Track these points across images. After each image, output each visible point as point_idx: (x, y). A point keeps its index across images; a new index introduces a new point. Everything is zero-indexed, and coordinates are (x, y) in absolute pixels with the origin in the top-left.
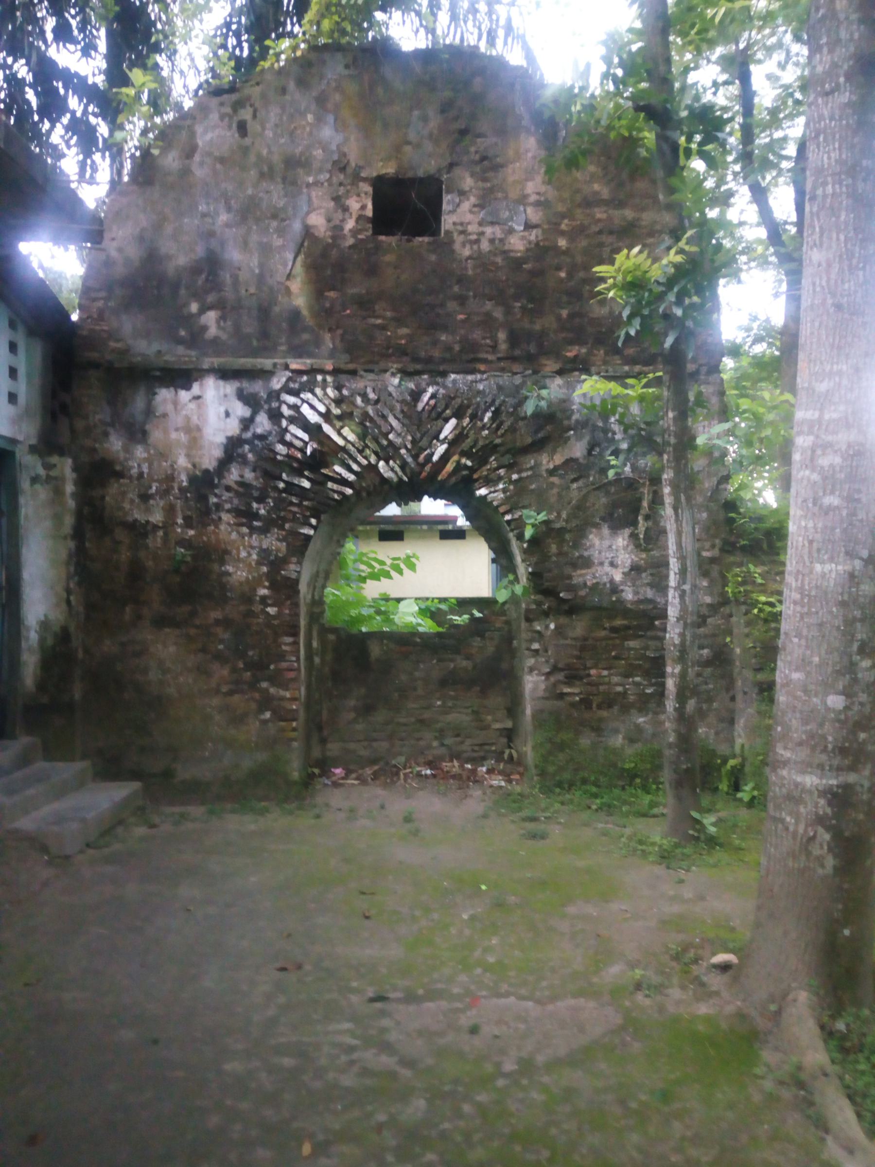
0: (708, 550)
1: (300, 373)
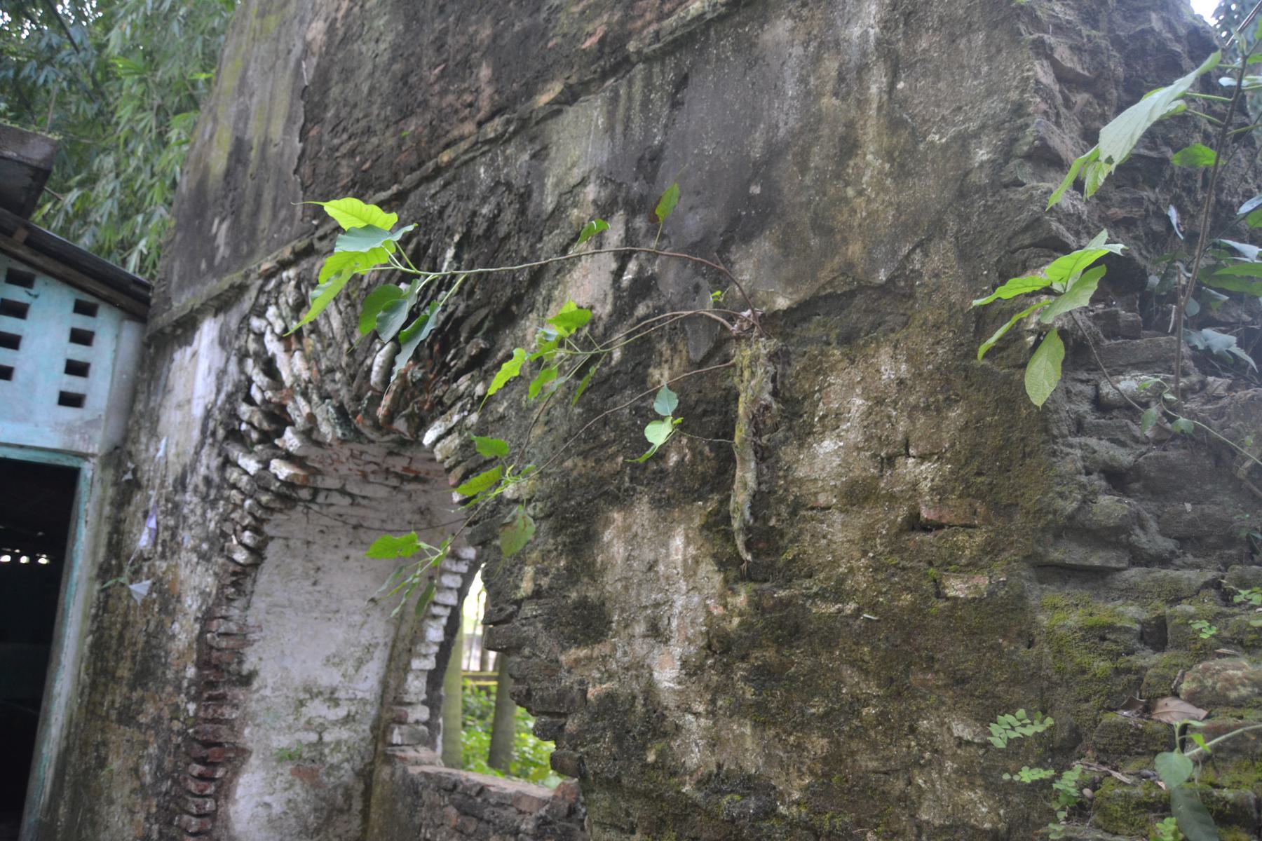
0: (973, 566)
1: (268, 275)
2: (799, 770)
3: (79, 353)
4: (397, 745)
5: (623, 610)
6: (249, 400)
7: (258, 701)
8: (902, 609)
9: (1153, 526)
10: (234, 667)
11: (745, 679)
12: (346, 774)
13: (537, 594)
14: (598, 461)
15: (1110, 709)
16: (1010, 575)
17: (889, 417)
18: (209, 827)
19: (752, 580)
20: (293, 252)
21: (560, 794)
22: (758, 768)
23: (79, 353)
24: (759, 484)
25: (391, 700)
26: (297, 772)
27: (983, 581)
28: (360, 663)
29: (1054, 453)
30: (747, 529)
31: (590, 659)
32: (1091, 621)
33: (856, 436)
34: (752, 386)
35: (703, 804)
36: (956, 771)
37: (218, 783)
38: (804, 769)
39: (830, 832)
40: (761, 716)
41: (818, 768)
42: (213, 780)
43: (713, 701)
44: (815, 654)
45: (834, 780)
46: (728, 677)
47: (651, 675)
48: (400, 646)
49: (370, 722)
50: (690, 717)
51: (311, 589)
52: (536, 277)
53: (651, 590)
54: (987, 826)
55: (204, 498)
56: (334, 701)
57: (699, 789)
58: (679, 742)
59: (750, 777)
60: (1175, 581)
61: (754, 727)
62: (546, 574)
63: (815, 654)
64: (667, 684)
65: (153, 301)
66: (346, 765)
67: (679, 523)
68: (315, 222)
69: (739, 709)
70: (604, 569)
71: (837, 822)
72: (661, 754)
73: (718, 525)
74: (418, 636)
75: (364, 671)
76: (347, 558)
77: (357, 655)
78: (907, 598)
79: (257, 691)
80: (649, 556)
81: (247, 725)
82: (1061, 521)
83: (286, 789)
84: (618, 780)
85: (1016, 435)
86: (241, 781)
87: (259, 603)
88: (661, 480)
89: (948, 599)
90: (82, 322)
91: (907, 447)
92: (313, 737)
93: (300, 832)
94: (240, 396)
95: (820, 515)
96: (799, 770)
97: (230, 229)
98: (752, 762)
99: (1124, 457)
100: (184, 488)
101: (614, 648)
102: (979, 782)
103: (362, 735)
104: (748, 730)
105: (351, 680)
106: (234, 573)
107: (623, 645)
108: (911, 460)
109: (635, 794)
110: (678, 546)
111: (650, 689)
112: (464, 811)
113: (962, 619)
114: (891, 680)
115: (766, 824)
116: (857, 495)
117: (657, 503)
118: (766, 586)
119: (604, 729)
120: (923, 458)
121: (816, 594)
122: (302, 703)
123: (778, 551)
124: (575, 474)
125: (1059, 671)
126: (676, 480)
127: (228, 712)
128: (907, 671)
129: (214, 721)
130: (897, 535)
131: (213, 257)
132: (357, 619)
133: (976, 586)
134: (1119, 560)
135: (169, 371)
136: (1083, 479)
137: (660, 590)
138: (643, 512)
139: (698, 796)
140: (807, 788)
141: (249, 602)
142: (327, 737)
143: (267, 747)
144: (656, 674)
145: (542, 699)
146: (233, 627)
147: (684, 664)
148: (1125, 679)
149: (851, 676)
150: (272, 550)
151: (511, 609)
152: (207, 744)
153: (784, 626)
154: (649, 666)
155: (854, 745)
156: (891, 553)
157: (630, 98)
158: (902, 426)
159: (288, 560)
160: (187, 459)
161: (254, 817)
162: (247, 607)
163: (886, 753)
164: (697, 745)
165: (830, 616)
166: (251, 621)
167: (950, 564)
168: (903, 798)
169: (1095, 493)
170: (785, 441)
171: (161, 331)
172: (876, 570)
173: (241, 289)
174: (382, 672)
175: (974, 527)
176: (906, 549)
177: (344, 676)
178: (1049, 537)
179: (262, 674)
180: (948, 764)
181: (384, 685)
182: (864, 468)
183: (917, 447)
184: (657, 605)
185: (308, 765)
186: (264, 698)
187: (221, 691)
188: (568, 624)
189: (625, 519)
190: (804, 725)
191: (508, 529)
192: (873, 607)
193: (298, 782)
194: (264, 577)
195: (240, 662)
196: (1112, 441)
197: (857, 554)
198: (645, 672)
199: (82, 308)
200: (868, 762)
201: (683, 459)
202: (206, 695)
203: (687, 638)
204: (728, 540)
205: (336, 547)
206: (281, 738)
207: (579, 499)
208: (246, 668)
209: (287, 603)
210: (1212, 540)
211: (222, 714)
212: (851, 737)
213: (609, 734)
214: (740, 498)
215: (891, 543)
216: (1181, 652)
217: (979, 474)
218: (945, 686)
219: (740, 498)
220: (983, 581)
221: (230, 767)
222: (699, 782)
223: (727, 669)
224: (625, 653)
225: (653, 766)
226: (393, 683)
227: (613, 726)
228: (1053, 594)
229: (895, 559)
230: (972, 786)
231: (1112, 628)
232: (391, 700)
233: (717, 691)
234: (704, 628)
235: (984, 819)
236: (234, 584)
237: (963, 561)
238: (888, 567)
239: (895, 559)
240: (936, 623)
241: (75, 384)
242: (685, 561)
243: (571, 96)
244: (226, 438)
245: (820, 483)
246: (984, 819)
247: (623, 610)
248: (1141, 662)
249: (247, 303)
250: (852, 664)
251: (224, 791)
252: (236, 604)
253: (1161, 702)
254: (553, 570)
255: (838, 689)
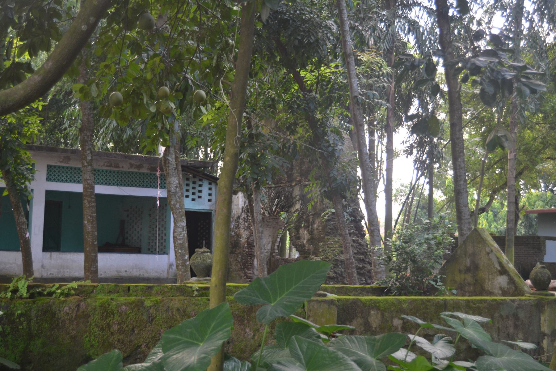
3: (210, 192)
23: (210, 192)
34: (311, 220)
52: (293, 204)
55: (244, 221)
74: (276, 240)
90: (210, 186)
107: (301, 240)
116: (317, 229)
153: (312, 238)
160: (240, 214)
199: (210, 184)
232: (273, 249)
241: (210, 198)
243: (296, 185)
251: (253, 261)
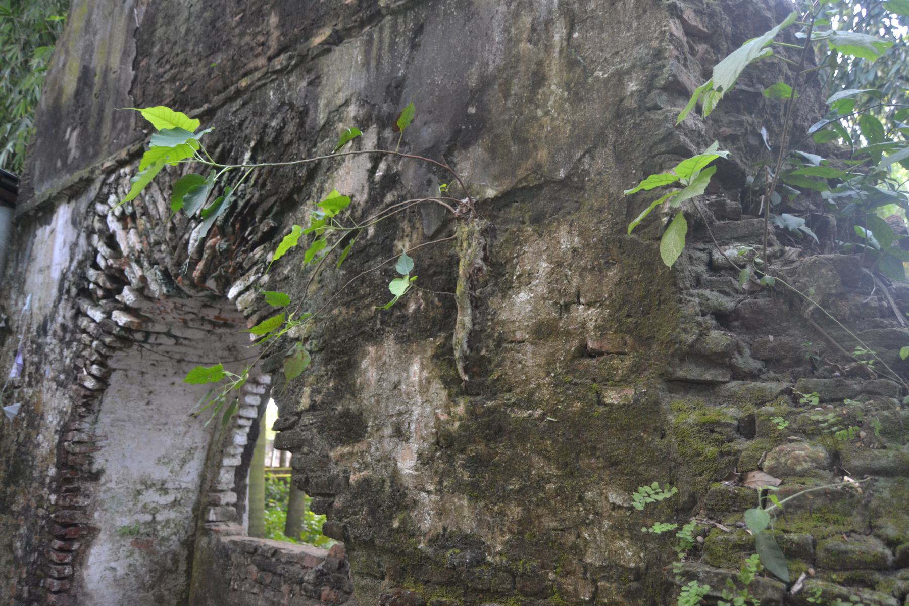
1: (109, 172)
2: (501, 530)
4: (213, 521)
5: (375, 418)
6: (96, 266)
7: (105, 492)
8: (574, 413)
9: (747, 352)
10: (86, 466)
11: (463, 466)
12: (174, 544)
13: (313, 407)
14: (357, 309)
15: (716, 481)
16: (649, 387)
17: (566, 276)
18: (68, 586)
19: (468, 394)
20: (128, 154)
21: (333, 553)
22: (472, 530)
24: (474, 325)
25: (208, 488)
26: (136, 543)
27: (630, 392)
28: (184, 462)
29: (680, 301)
30: (465, 358)
31: (351, 454)
32: (704, 419)
33: (542, 290)
34: (469, 254)
35: (433, 556)
36: (611, 527)
37: (74, 553)
38: (505, 529)
39: (523, 573)
40: (475, 492)
41: (515, 528)
42: (71, 551)
43: (440, 483)
44: (513, 447)
45: (526, 536)
46: (451, 465)
47: (396, 465)
48: (214, 448)
49: (192, 505)
50: (424, 494)
51: (145, 407)
53: (396, 403)
54: (632, 565)
55: (61, 340)
56: (164, 491)
57: (430, 546)
58: (416, 512)
59: (466, 535)
60: (762, 390)
61: (470, 500)
62: (320, 393)
63: (513, 447)
64: (407, 471)
65: (20, 191)
66: (173, 537)
67: (416, 354)
68: (145, 131)
69: (459, 488)
70: (362, 388)
71: (528, 566)
72: (403, 522)
73: (444, 355)
74: (228, 441)
75: (187, 467)
76: (173, 384)
77: (182, 456)
78: (578, 405)
79: (104, 484)
80: (394, 378)
81: (97, 510)
82: (685, 349)
83: (127, 557)
84: (372, 541)
85: (654, 288)
86: (92, 551)
87: (105, 419)
88: (403, 322)
89: (606, 405)
91: (578, 297)
92: (148, 517)
93: (139, 588)
94: (89, 263)
95: (517, 347)
96: (501, 530)
97: (80, 135)
98: (468, 525)
99: (728, 303)
100: (46, 333)
101: (369, 446)
102: (627, 534)
103: (186, 515)
104: (465, 503)
105: (177, 475)
106: (85, 397)
108: (581, 307)
109: (384, 551)
110: (415, 370)
111: (395, 475)
112: (262, 568)
113: (616, 419)
114: (566, 464)
115: (478, 569)
116: (543, 332)
117: (400, 340)
118: (479, 398)
119: (362, 505)
120: (589, 305)
121: (514, 404)
122: (139, 493)
123: (488, 373)
124: (341, 318)
125: (683, 455)
126: (414, 323)
127: (81, 501)
128: (577, 458)
129: (70, 507)
130: (572, 360)
131: (67, 158)
132: (182, 429)
133: (626, 396)
134: (724, 375)
135: (33, 244)
136: (700, 319)
137: (403, 403)
138: (390, 346)
139: (430, 551)
140: (507, 542)
141: (97, 418)
142: (159, 517)
143: (112, 526)
144: (399, 464)
145: (317, 484)
146: (84, 437)
147: (420, 456)
148: (726, 459)
149: (538, 461)
150: (114, 379)
151: (293, 419)
152: (65, 525)
153: (491, 427)
154: (394, 458)
155: (540, 511)
156: (567, 373)
157: (381, 41)
158: (575, 282)
159: (127, 386)
160: (48, 311)
161: (103, 578)
162: (96, 421)
163: (563, 516)
164: (429, 514)
165: (524, 419)
166: (99, 432)
167: (607, 380)
168: (574, 548)
169: (708, 329)
170: (492, 294)
171: (26, 214)
172: (556, 386)
173: (87, 182)
174: (200, 468)
175: (625, 354)
176: (577, 371)
177: (171, 472)
178: (677, 360)
179: (108, 472)
180: (606, 523)
181: (203, 478)
182: (548, 312)
183: (585, 297)
184: (400, 414)
185: (145, 538)
186: (109, 489)
187: (76, 485)
188: (336, 429)
189: (377, 352)
190: (505, 498)
191: (290, 359)
192: (554, 412)
193: (137, 551)
194: (109, 399)
195: (91, 463)
196: (721, 292)
197: (543, 374)
198: (392, 462)
200: (550, 523)
201: (419, 307)
202: (64, 489)
203: (422, 438)
204: (451, 366)
205: (164, 376)
206: (123, 519)
207: (343, 337)
208: (95, 467)
209: (126, 418)
210: (787, 361)
211: (77, 502)
212: (538, 505)
213: (365, 508)
214: (460, 335)
215: (567, 366)
216: (764, 440)
217: (628, 316)
218: (604, 467)
219: (460, 335)
220: (630, 392)
221: (83, 541)
222: (430, 541)
223: (450, 459)
224: (377, 449)
225: (398, 531)
226: (209, 476)
227: (368, 502)
228: (679, 401)
229: (570, 378)
230: (622, 537)
231: (718, 423)
232: (207, 488)
233: (443, 475)
234: (434, 430)
235: (630, 560)
236: (84, 405)
237: (617, 378)
238: (565, 383)
239: (570, 378)
240: (598, 422)
242: (420, 381)
243: (337, 39)
244: (78, 295)
245: (517, 324)
246: (630, 560)
247: (375, 418)
248: (737, 447)
249: (93, 193)
250: (539, 453)
251: (79, 560)
252: (87, 420)
253: (751, 475)
254: (325, 390)
255: (529, 472)
